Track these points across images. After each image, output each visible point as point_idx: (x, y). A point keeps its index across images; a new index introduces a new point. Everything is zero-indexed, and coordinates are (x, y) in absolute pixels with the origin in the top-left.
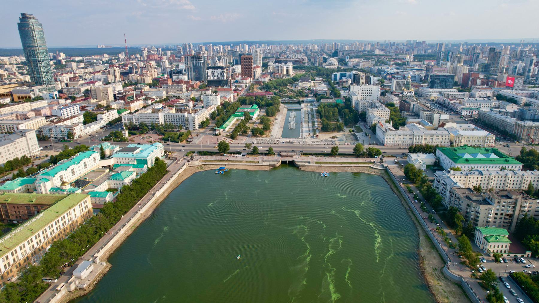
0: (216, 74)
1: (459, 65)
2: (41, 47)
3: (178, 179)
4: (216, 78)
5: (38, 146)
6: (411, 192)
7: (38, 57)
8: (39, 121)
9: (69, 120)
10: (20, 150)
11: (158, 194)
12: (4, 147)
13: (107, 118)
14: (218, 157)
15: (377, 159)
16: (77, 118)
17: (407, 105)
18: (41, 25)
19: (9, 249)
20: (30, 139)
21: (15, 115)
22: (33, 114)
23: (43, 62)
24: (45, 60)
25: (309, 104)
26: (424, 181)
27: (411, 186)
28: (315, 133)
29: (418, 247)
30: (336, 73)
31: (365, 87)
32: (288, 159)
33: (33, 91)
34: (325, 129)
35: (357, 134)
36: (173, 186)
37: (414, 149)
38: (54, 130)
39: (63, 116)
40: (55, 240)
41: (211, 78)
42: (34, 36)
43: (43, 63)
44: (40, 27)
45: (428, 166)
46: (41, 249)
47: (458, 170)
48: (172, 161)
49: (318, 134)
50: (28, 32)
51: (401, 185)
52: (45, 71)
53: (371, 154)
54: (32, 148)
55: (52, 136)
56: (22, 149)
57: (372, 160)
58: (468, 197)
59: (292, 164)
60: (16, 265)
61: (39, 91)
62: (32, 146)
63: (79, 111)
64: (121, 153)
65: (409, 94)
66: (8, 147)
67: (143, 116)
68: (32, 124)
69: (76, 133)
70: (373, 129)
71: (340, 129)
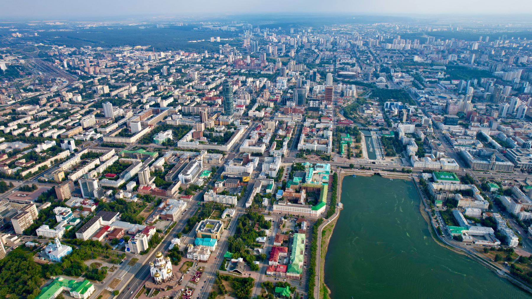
0: (315, 104)
1: (468, 102)
4: (315, 106)
6: (420, 188)
14: (350, 170)
15: (411, 174)
17: (427, 141)
25: (375, 132)
26: (425, 185)
27: (421, 186)
28: (383, 157)
29: (420, 204)
30: (388, 102)
31: (406, 125)
32: (377, 172)
34: (388, 155)
35: (402, 159)
37: (425, 172)
41: (311, 106)
45: (429, 179)
47: (437, 182)
49: (385, 158)
51: (418, 186)
53: (408, 172)
57: (408, 174)
58: (435, 192)
59: (378, 174)
65: (430, 131)
70: (410, 157)
71: (393, 155)
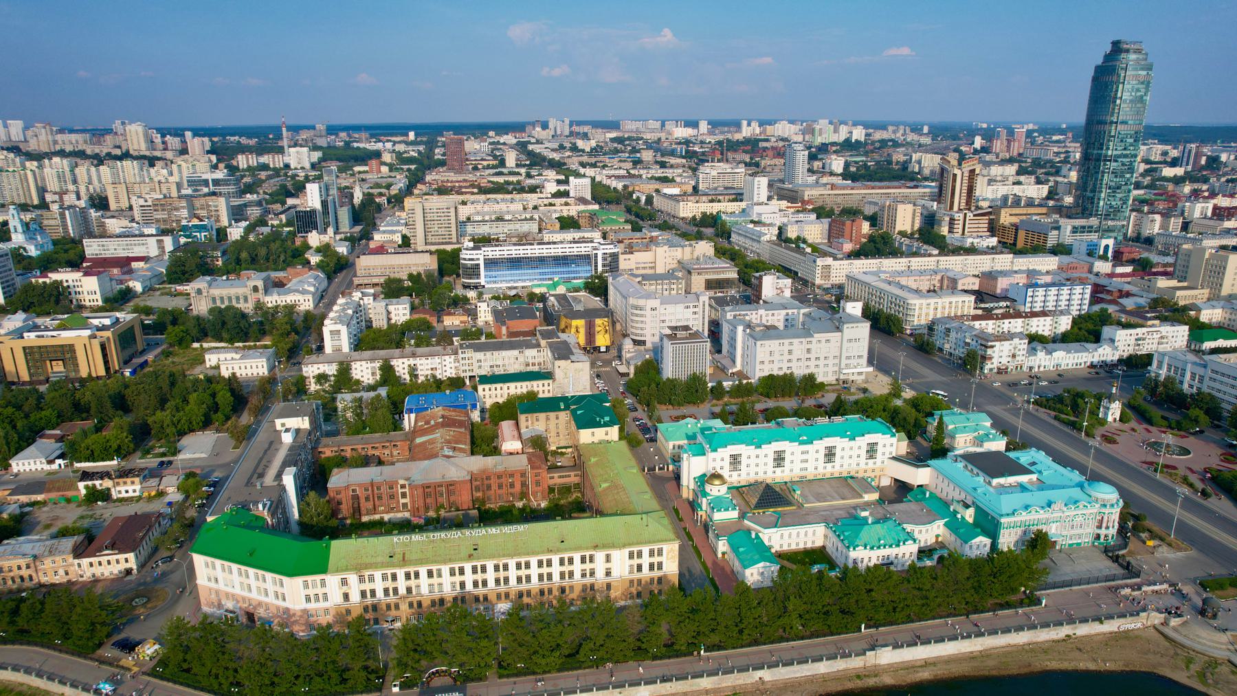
2: (1123, 123)
3: (1045, 651)
5: (864, 361)
7: (1108, 149)
8: (954, 304)
9: (1020, 321)
10: (817, 358)
11: (886, 657)
12: (781, 341)
13: (1133, 342)
16: (1048, 319)
18: (1149, 68)
19: (404, 562)
20: (850, 341)
21: (939, 277)
22: (974, 284)
23: (1116, 161)
24: (1126, 156)
33: (1058, 228)
36: (991, 663)
38: (953, 335)
39: (1028, 305)
40: (526, 600)
42: (1119, 95)
43: (1116, 164)
44: (1144, 73)
46: (481, 599)
48: (1119, 571)
50: (1107, 87)
52: (1113, 184)
54: (848, 362)
55: (947, 346)
56: (822, 359)
60: (410, 599)
61: (1075, 230)
62: (848, 358)
63: (1087, 302)
64: (960, 465)
66: (791, 344)
67: (1223, 375)
68: (932, 307)
69: (991, 358)
